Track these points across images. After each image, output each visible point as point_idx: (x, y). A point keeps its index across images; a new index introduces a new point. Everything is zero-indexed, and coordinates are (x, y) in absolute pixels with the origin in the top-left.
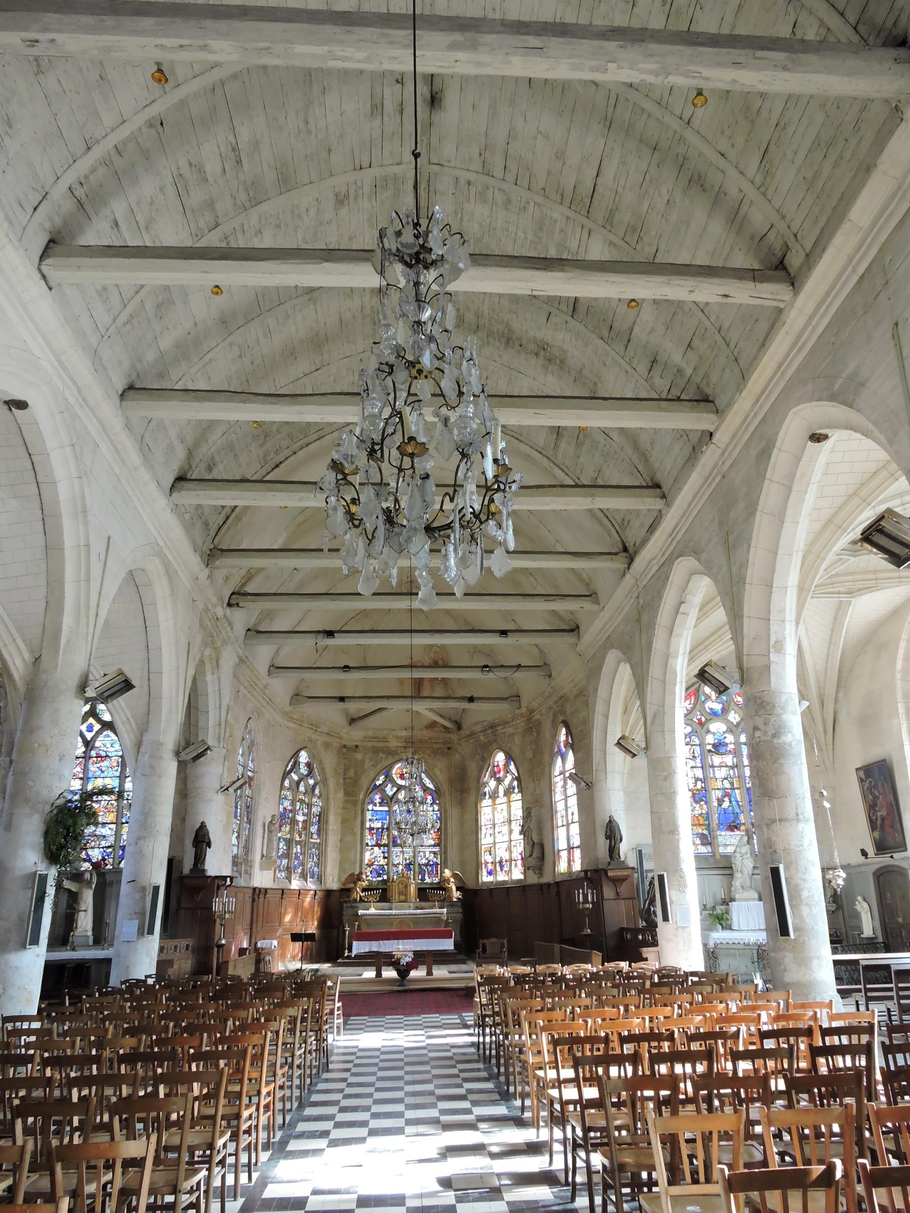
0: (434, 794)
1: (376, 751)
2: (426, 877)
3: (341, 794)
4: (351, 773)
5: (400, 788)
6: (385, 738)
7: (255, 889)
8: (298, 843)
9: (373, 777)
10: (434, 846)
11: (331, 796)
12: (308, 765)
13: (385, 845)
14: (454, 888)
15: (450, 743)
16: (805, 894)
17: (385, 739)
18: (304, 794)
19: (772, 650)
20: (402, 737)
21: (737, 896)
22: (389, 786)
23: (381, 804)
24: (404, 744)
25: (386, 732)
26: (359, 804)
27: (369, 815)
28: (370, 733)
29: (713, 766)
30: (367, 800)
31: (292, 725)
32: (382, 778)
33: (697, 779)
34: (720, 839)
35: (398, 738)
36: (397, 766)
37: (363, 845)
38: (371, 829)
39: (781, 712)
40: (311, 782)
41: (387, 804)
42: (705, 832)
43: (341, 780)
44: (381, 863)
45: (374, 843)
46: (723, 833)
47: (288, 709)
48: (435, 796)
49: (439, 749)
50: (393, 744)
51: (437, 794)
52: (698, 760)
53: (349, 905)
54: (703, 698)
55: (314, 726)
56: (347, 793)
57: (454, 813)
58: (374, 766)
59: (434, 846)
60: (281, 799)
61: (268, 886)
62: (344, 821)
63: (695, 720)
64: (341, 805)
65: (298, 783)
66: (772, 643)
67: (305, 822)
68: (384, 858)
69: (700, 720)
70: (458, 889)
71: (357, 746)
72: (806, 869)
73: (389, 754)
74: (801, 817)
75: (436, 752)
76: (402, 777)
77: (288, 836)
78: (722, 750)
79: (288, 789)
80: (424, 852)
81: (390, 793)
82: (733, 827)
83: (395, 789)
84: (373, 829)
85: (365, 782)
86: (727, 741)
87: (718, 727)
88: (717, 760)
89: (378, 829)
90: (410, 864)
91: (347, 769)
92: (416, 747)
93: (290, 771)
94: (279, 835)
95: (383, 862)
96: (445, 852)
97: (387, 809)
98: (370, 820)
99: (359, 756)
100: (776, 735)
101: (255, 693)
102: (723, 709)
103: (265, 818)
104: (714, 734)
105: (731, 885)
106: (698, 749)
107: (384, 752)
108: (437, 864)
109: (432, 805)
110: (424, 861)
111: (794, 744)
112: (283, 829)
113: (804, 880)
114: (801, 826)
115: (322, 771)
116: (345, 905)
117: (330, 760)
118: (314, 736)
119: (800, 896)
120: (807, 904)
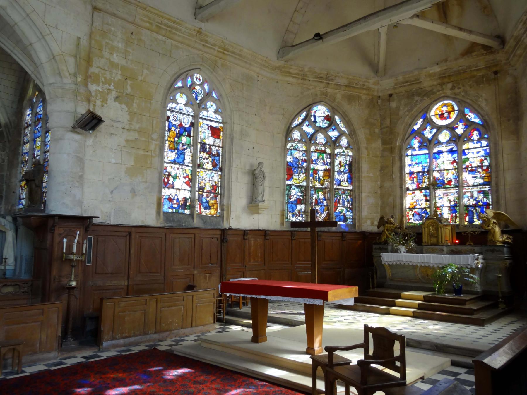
0: (480, 128)
1: (410, 95)
3: (378, 144)
4: (388, 122)
5: (440, 129)
6: (416, 80)
7: (223, 231)
8: (317, 190)
9: (409, 121)
10: (483, 185)
11: (363, 145)
12: (327, 118)
13: (426, 189)
14: (497, 230)
15: (496, 65)
17: (417, 81)
18: (324, 145)
20: (435, 74)
22: (429, 128)
23: (420, 148)
24: (439, 81)
25: (416, 73)
26: (397, 151)
27: (408, 160)
28: (400, 78)
30: (404, 147)
31: (291, 80)
32: (420, 122)
35: (430, 75)
36: (436, 107)
37: (403, 191)
38: (411, 173)
40: (333, 134)
41: (427, 147)
43: (377, 131)
44: (423, 206)
45: (415, 187)
47: (281, 63)
48: (482, 130)
49: (483, 76)
50: (427, 84)
51: (484, 129)
53: (377, 246)
55: (326, 79)
56: (384, 143)
57: (507, 145)
58: (409, 111)
59: (483, 185)
61: (272, 228)
62: (382, 169)
64: (379, 154)
65: (313, 136)
67: (326, 170)
68: (427, 201)
70: (503, 232)
71: (391, 95)
73: (424, 95)
75: (479, 82)
76: (442, 116)
77: (304, 184)
79: (299, 141)
80: (472, 193)
83: (435, 130)
85: (400, 128)
89: (419, 172)
90: (455, 205)
91: (383, 119)
92: (453, 83)
95: (424, 205)
96: (497, 191)
97: (426, 152)
98: (410, 165)
99: (394, 104)
101: (176, 37)
107: (419, 95)
108: (487, 205)
109: (479, 141)
110: (472, 202)
112: (295, 177)
115: (348, 123)
116: (374, 247)
117: (357, 112)
118: (330, 90)
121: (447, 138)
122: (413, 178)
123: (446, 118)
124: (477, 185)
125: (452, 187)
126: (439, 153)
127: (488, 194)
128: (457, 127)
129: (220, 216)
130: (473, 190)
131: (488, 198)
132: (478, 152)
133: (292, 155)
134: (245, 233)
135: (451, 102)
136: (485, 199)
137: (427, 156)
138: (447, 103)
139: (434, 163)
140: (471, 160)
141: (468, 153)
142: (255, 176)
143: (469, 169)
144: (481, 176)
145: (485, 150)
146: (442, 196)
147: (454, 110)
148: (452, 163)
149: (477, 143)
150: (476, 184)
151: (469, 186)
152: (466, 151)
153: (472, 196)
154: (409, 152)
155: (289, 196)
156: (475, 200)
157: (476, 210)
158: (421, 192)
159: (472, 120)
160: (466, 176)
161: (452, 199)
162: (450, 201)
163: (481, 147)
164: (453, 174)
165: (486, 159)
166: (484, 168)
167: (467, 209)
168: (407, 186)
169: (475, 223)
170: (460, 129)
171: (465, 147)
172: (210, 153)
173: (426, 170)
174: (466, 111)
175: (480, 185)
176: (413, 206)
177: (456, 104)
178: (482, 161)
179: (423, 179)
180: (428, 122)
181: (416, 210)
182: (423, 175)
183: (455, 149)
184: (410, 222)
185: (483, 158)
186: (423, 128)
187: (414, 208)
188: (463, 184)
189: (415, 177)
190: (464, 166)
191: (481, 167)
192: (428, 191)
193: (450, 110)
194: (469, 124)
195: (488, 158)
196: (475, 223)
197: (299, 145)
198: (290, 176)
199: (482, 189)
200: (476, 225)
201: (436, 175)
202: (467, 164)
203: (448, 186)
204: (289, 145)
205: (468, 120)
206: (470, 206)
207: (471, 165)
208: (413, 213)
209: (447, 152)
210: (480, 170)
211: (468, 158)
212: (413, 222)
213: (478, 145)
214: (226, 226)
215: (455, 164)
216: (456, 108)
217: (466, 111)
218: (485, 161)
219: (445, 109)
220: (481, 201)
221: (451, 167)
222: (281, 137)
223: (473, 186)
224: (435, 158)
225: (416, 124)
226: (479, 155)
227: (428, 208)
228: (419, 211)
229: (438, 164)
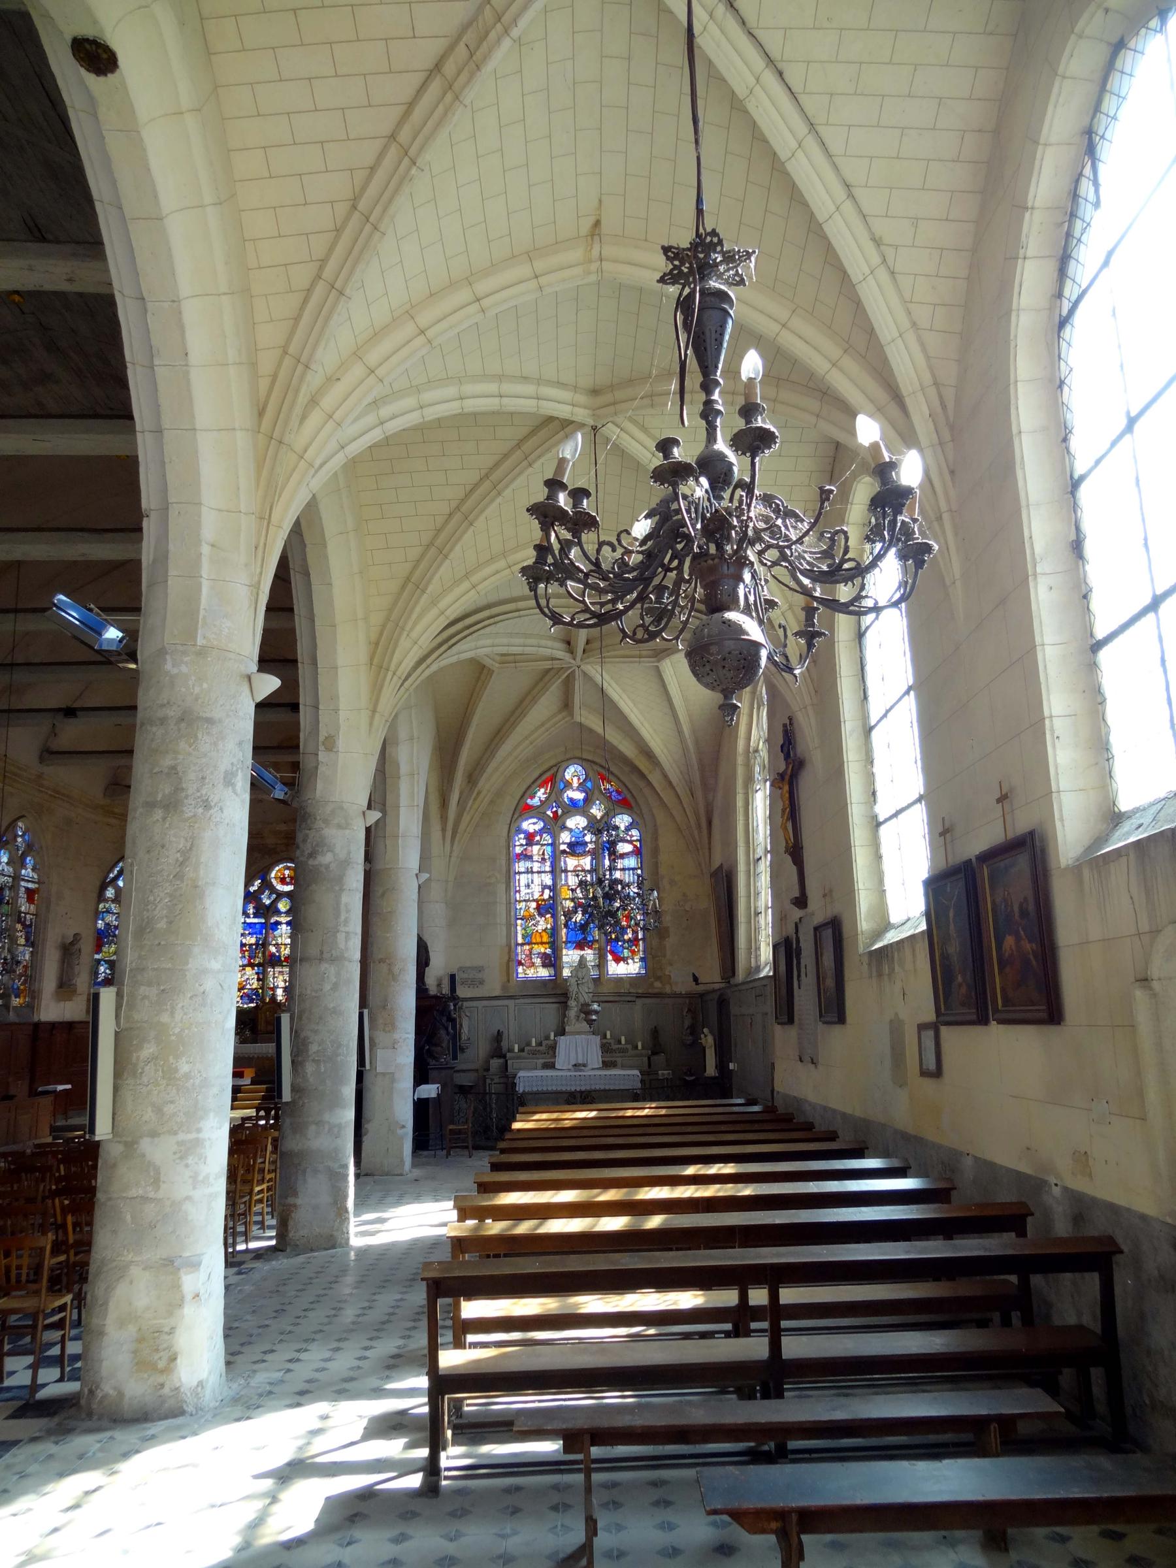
5: (280, 895)
7: (37, 1026)
13: (259, 965)
16: (314, 1048)
19: (321, 748)
21: (567, 1029)
29: (566, 871)
33: (544, 887)
34: (565, 959)
39: (323, 825)
42: (548, 951)
46: (571, 952)
52: (548, 864)
54: (562, 786)
60: (97, 914)
63: (549, 813)
66: (321, 738)
68: (259, 980)
69: (555, 813)
72: (321, 1018)
74: (326, 956)
76: (283, 881)
78: (579, 850)
79: (113, 901)
81: (268, 902)
82: (580, 946)
83: (274, 896)
86: (588, 838)
87: (577, 822)
88: (571, 863)
89: (251, 945)
93: (116, 878)
94: (97, 957)
100: (312, 855)
102: (586, 800)
103: (63, 937)
104: (571, 830)
105: (564, 1016)
106: (549, 849)
111: (333, 866)
112: (104, 949)
113: (316, 1032)
114: (324, 966)
119: (307, 1051)
120: (313, 1060)
123: (287, 884)
126: (278, 923)
129: (28, 1006)
133: (103, 920)
134: (53, 1026)
142: (69, 950)
155: (96, 973)
162: (285, 981)
172: (24, 924)
186: (260, 890)
197: (113, 906)
198: (98, 950)
201: (273, 949)
204: (101, 906)
214: (36, 1019)
219: (287, 872)
222: (95, 895)
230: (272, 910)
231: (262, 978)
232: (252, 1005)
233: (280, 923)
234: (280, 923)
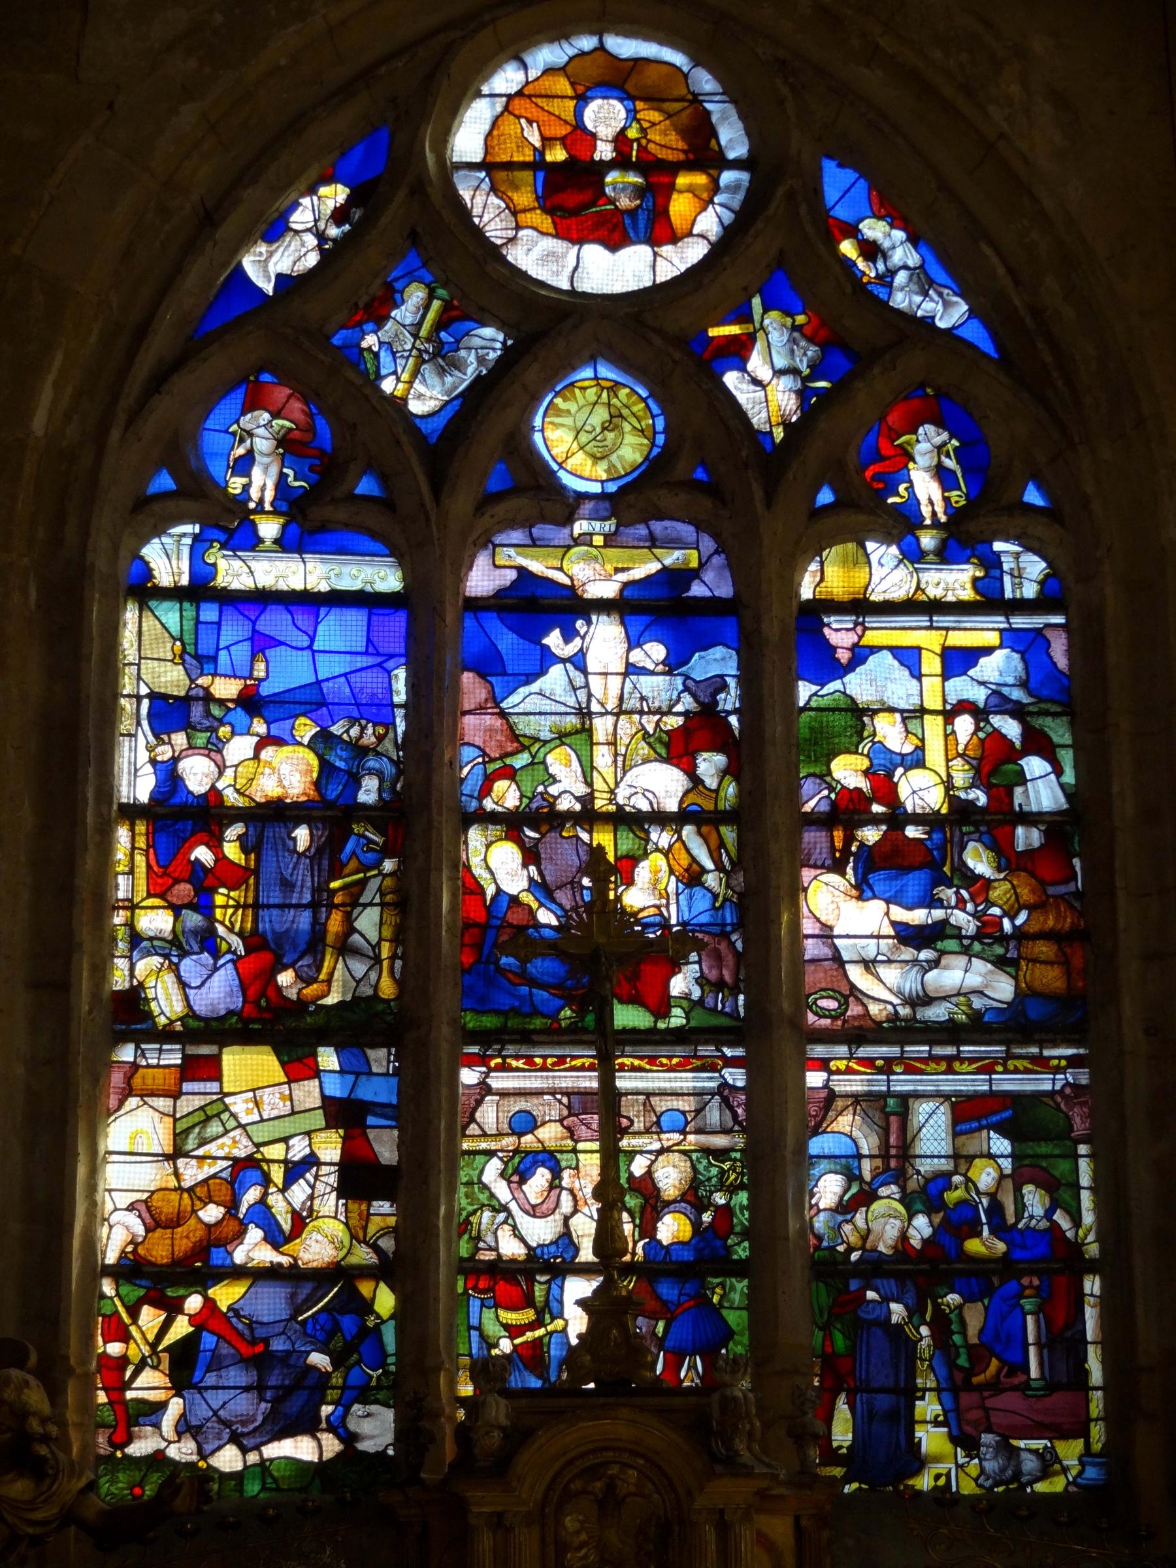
2: (931, 1439)
10: (1012, 1027)
13: (355, 1027)
27: (148, 652)
36: (507, 79)
38: (180, 817)
44: (317, 1248)
45: (218, 991)
68: (358, 1179)
76: (572, 196)
81: (426, 398)
83: (488, 340)
84: (208, 815)
89: (272, 816)
90: (707, 1254)
110: (888, 1223)
121: (631, 451)
122: (204, 883)
124: (950, 1032)
125: (678, 1036)
127: (1066, 1138)
128: (736, 352)
130: (902, 1083)
131: (1061, 1192)
132: (958, 661)
135: (677, 58)
136: (1035, 1201)
137: (397, 623)
138: (638, 63)
139: (476, 727)
140: (889, 732)
141: (860, 654)
143: (871, 835)
144: (988, 931)
145: (1029, 645)
146: (550, 1134)
147: (704, 155)
148: (678, 749)
149: (945, 556)
150: (937, 1013)
151: (859, 1033)
152: (839, 634)
153: (897, 1156)
154: (167, 559)
156: (926, 1196)
157: (942, 1325)
158: (299, 1066)
159: (900, 300)
160: (839, 911)
161: (670, 1177)
163: (989, 600)
164: (693, 877)
165: (1037, 743)
166: (1026, 837)
167: (846, 1308)
168: (119, 980)
169: (924, 1482)
170: (766, 387)
171: (824, 577)
173: (368, 792)
174: (838, 183)
175: (976, 1026)
176: (185, 1239)
177: (734, 94)
178: (994, 763)
179: (321, 902)
180: (409, 223)
181: (226, 1295)
182: (328, 856)
183: (715, 584)
184: (139, 1448)
185: (1011, 728)
186: (349, 283)
187: (202, 1265)
188: (802, 1003)
189: (226, 874)
190: (814, 801)
191: (989, 813)
192: (380, 1058)
193: (665, 141)
194: (857, 343)
195: (1059, 732)
196: (924, 1482)
199: (1007, 1083)
200: (943, 1495)
202: (848, 771)
203: (627, 1016)
205: (868, 299)
206: (875, 1267)
207: (885, 788)
208: (181, 1328)
209: (621, 607)
210: (979, 861)
211: (858, 714)
212: (183, 1451)
213: (956, 581)
215: (709, 764)
216: (732, 138)
217: (838, 183)
218: (1034, 765)
219: (605, 117)
220: (996, 1209)
221: (663, 785)
223: (899, 1030)
224: (489, 665)
225: (276, 230)
226: (962, 688)
227: (384, 1271)
228: (270, 1304)
229: (520, 742)
230: (475, 472)
231: (402, 1166)
232: (300, 1449)
233: (570, 608)
234: (570, 608)
